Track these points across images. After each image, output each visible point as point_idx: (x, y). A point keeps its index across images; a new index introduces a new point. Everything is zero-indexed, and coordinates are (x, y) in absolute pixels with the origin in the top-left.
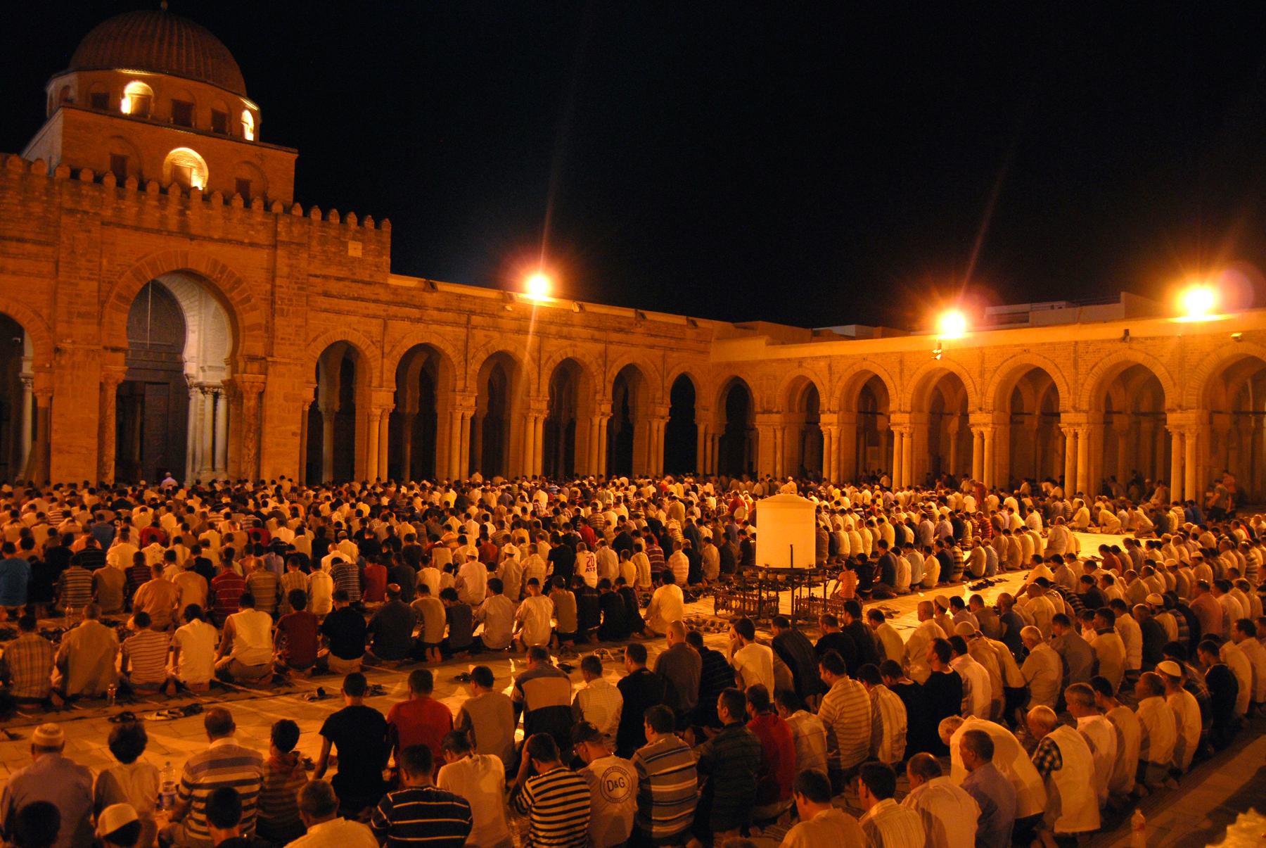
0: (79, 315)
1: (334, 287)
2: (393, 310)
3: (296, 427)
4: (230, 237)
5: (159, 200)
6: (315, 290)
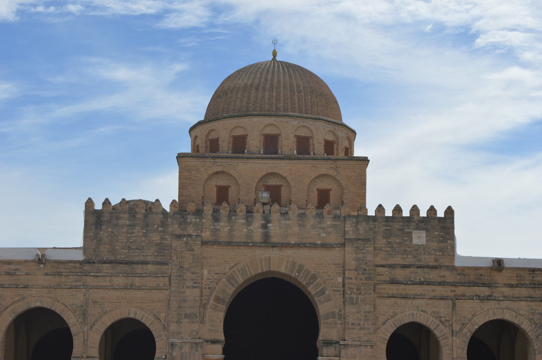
0: (186, 316)
1: (400, 274)
2: (461, 290)
4: (305, 241)
5: (247, 218)
6: (382, 278)
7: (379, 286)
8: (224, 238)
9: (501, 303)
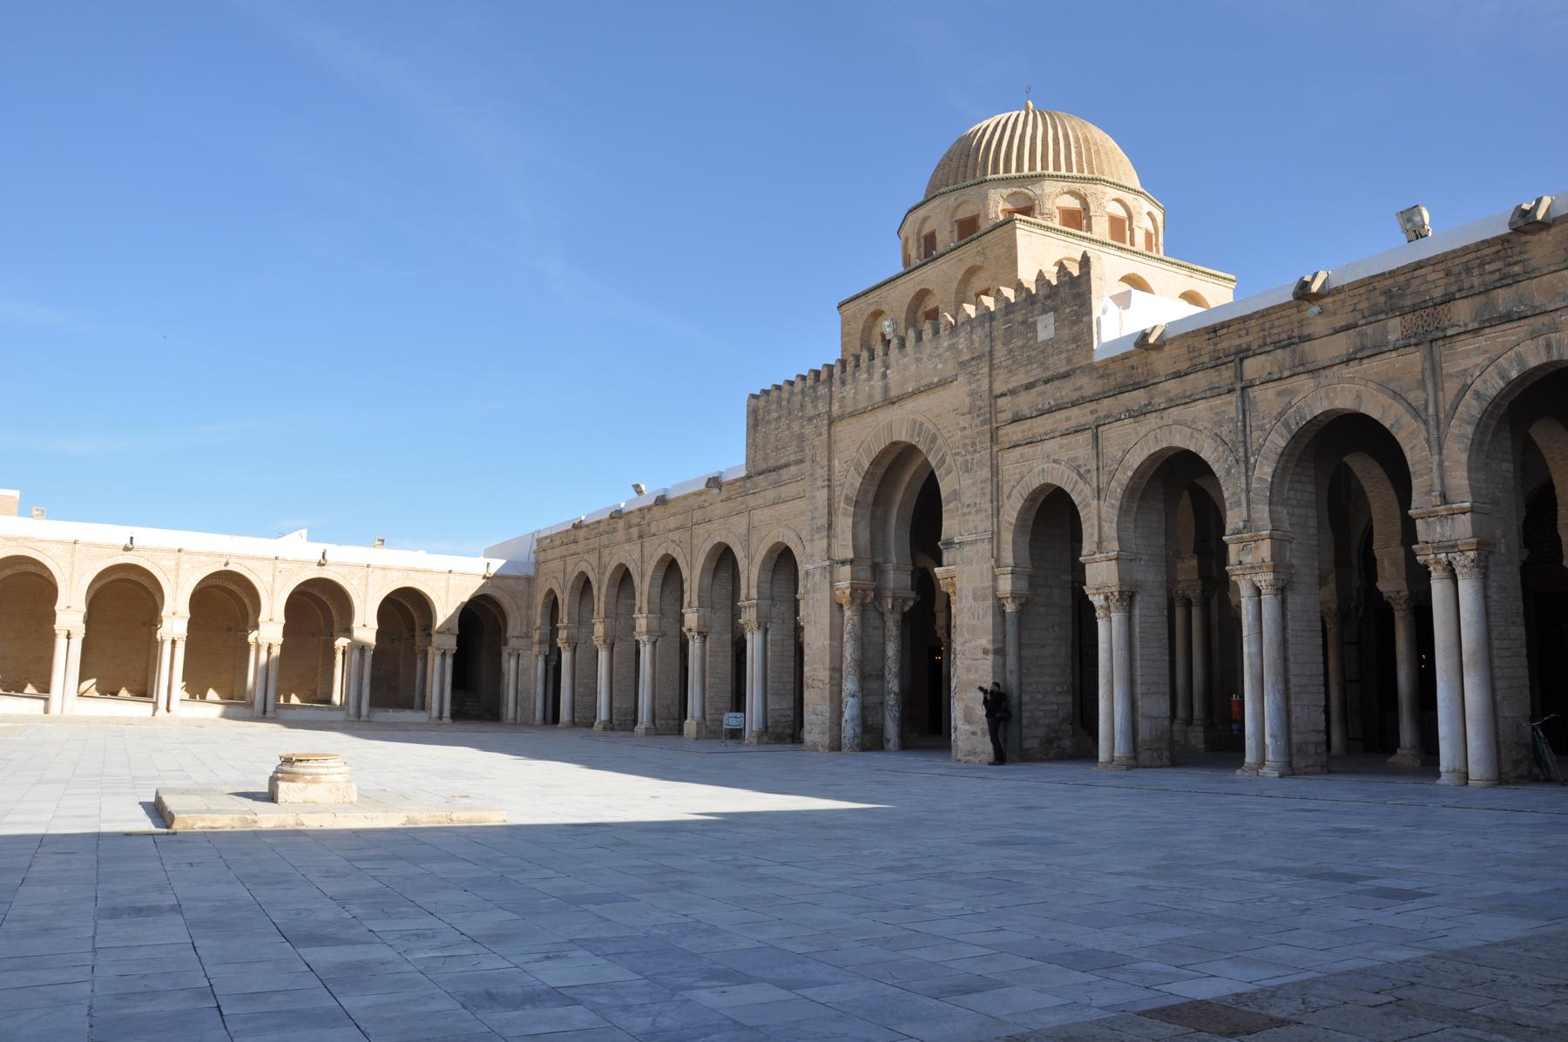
1: (1025, 402)
3: (986, 641)
7: (1001, 432)
8: (849, 410)
9: (1165, 414)
